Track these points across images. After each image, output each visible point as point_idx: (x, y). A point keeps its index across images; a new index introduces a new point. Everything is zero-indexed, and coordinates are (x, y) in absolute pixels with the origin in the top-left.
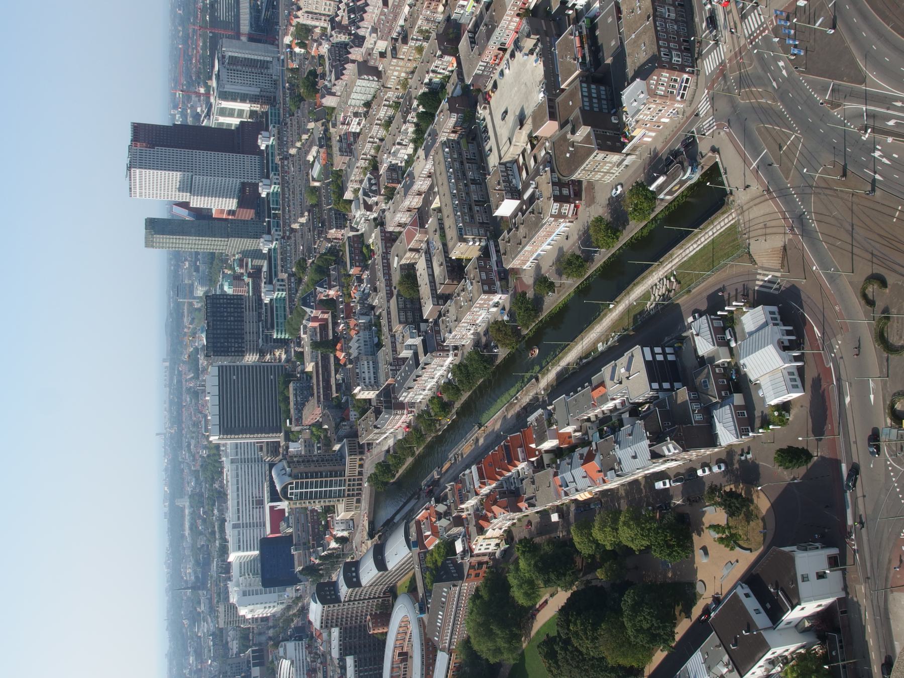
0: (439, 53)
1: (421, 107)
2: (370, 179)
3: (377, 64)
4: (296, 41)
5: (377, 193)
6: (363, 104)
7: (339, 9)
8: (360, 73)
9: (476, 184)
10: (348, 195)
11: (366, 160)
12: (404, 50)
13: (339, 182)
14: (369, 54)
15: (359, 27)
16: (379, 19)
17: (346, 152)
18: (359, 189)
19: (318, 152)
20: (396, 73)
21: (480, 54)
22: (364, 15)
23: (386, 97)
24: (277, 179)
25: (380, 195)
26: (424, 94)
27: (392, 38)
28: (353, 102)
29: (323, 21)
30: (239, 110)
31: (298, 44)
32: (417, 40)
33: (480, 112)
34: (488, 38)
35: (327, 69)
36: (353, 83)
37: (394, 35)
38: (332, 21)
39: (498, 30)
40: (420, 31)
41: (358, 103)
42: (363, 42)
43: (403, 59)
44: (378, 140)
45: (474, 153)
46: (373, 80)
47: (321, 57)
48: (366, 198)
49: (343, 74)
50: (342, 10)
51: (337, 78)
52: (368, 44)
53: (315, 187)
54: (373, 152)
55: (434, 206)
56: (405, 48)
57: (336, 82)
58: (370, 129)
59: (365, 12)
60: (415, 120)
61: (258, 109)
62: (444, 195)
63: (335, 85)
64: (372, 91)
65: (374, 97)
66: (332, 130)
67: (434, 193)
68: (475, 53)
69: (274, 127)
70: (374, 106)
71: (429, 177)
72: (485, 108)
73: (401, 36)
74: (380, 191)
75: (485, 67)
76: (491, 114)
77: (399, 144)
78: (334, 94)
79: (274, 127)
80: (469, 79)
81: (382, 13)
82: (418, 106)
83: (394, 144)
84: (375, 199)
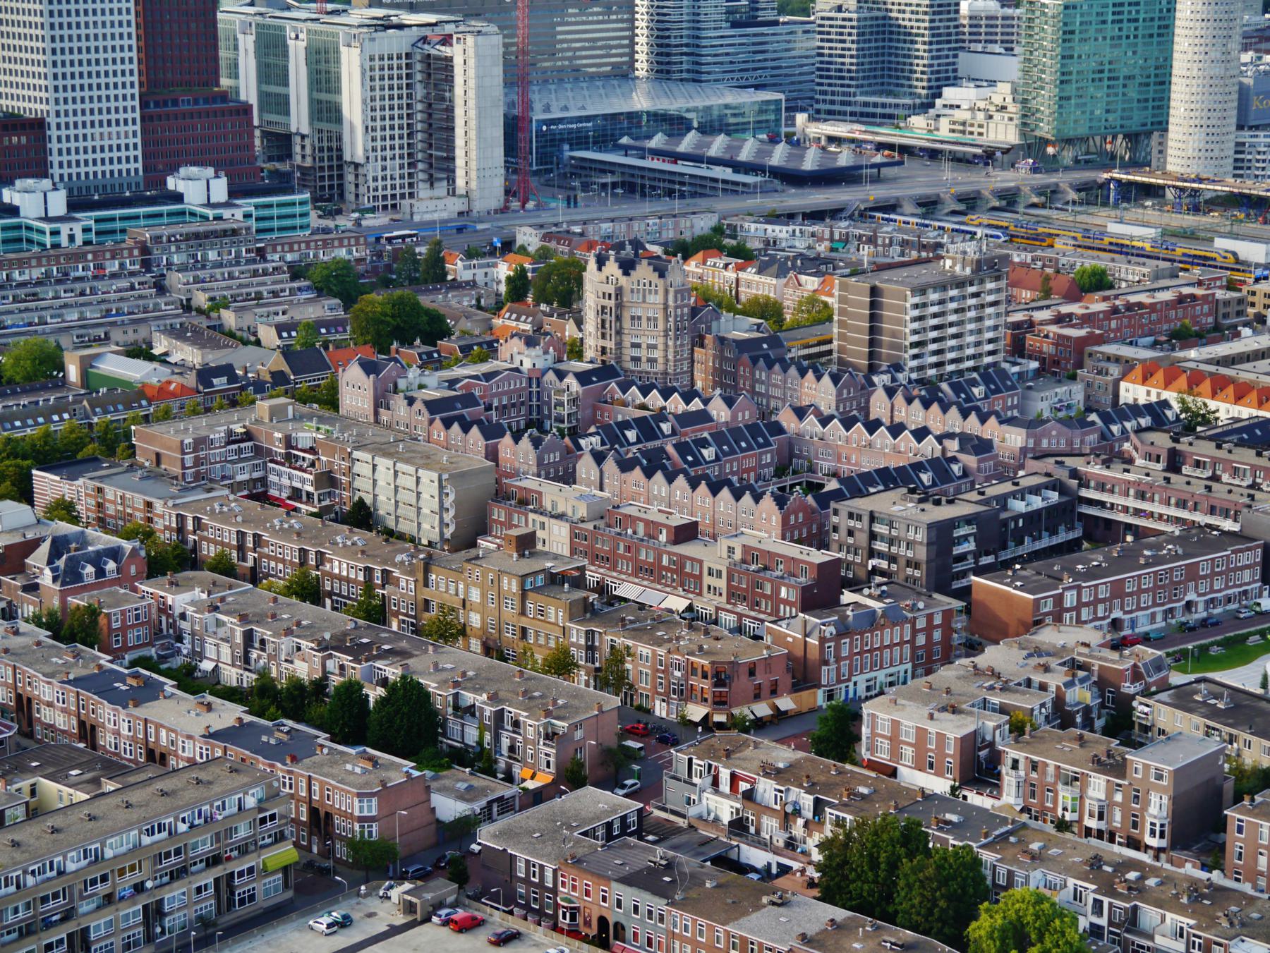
0: (561, 725)
1: (381, 691)
2: (115, 553)
3: (496, 530)
4: (527, 266)
5: (69, 577)
6: (361, 500)
7: (645, 391)
8: (459, 478)
9: (147, 923)
10: (47, 484)
11: (181, 530)
12: (552, 611)
13: (90, 449)
14: (523, 502)
15: (599, 458)
16: (633, 520)
17: (198, 462)
18: (75, 520)
19: (182, 367)
20: (475, 595)
21: (577, 862)
22: (637, 473)
23: (397, 573)
24: (72, 238)
25: (63, 595)
26: (423, 696)
27: (582, 569)
28: (363, 469)
29: (601, 343)
30: (287, 97)
31: (522, 273)
32: (590, 648)
33: (395, 894)
34: (628, 881)
35: (458, 372)
36: (427, 461)
37: (592, 576)
38: (606, 371)
39: (659, 904)
40: (618, 656)
41: (363, 484)
42: (557, 479)
43: (523, 612)
44: (250, 563)
45: (252, 898)
46: (442, 524)
47: (490, 350)
48: (45, 548)
49: (447, 424)
50: (640, 399)
51: (433, 407)
52: (553, 494)
53: (61, 368)
54: (209, 551)
55: (50, 788)
56: (556, 613)
57: (418, 405)
58: (285, 533)
59: (649, 474)
60: (336, 680)
61: (298, 159)
62: (92, 818)
63: (411, 401)
64: (406, 527)
65: (390, 534)
66: (263, 406)
67: (96, 782)
68: (577, 842)
69: (247, 216)
70: (360, 537)
71: (150, 754)
72: (409, 908)
73: (593, 597)
74: (74, 592)
75: (541, 885)
76: (394, 931)
77: (248, 637)
78: (380, 402)
79: (247, 216)
80: (495, 837)
81: (653, 528)
82: (384, 682)
83: (243, 619)
84: (46, 578)
